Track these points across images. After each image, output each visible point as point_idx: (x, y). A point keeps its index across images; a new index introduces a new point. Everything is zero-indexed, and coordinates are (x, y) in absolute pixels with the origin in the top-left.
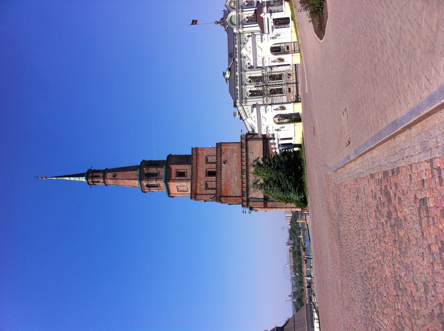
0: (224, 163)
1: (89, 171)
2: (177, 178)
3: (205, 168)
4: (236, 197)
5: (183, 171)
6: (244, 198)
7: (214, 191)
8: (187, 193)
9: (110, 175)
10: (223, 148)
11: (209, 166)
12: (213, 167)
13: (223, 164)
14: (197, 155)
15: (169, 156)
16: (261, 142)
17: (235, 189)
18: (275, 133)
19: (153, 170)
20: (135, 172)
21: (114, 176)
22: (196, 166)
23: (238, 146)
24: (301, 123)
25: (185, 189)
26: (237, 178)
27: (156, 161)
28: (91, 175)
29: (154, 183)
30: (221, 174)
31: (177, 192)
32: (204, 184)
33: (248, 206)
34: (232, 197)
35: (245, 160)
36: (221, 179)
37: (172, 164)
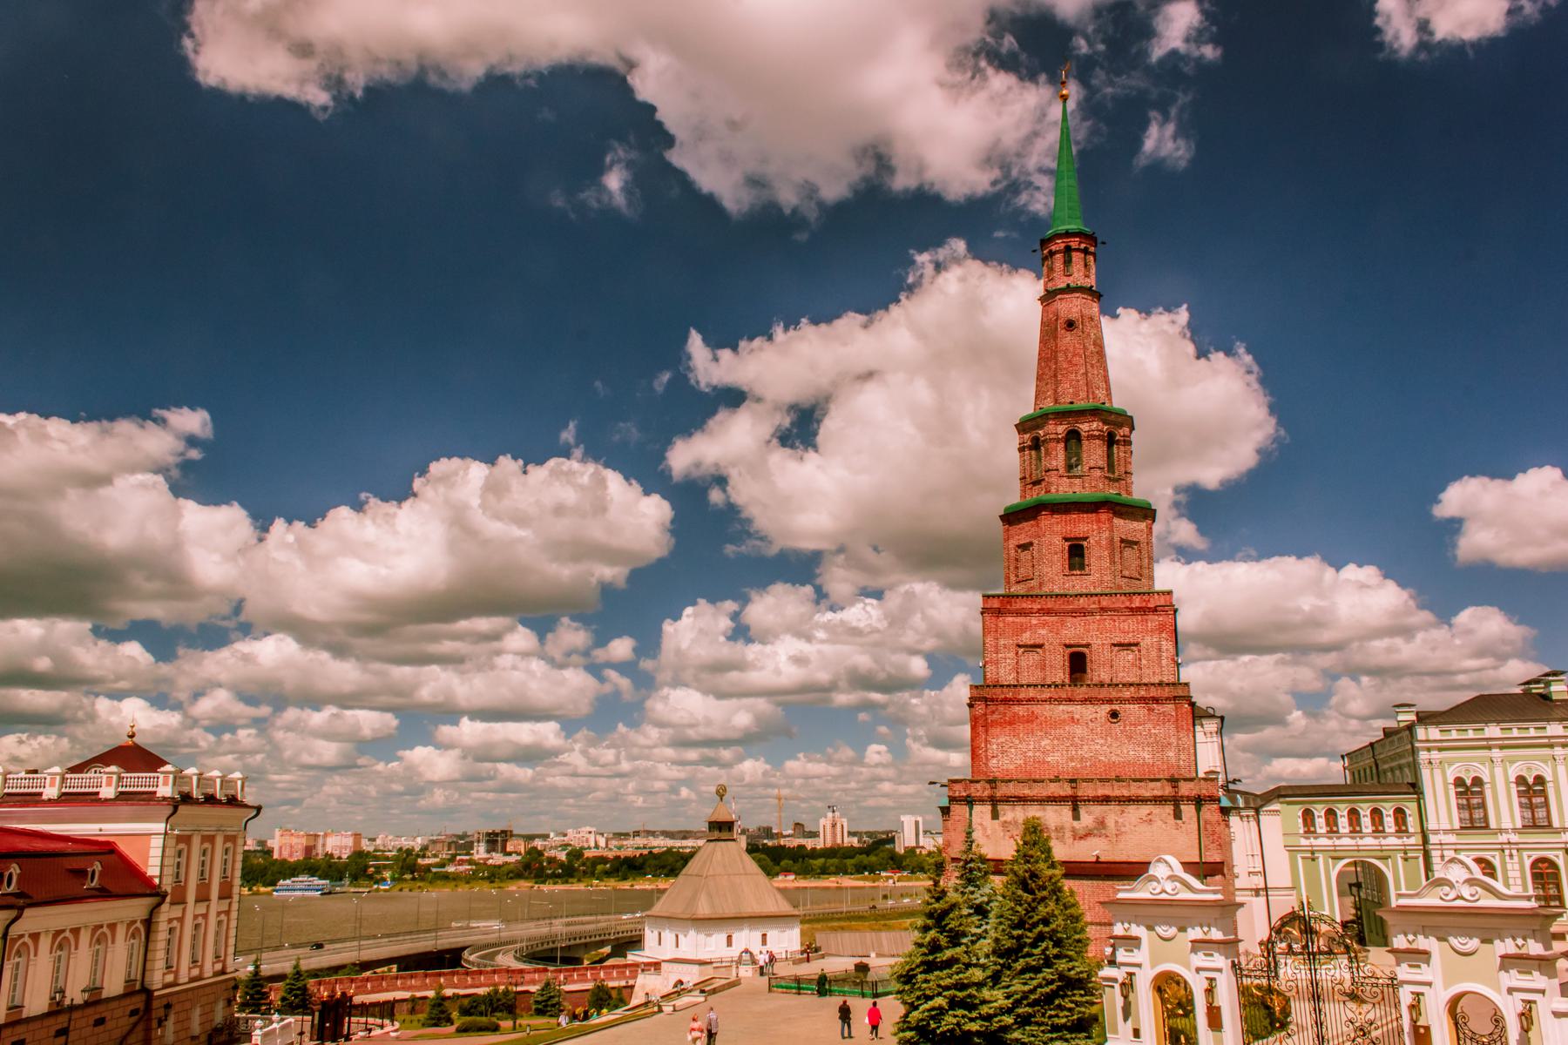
0: (1114, 714)
3: (1096, 643)
6: (978, 786)
8: (1013, 578)
10: (1169, 708)
12: (1099, 672)
13: (1107, 708)
14: (1143, 610)
15: (1146, 513)
19: (1094, 454)
20: (1083, 394)
21: (1070, 325)
28: (1074, 245)
30: (1070, 700)
32: (1039, 641)
33: (952, 799)
35: (1117, 793)
36: (1050, 700)
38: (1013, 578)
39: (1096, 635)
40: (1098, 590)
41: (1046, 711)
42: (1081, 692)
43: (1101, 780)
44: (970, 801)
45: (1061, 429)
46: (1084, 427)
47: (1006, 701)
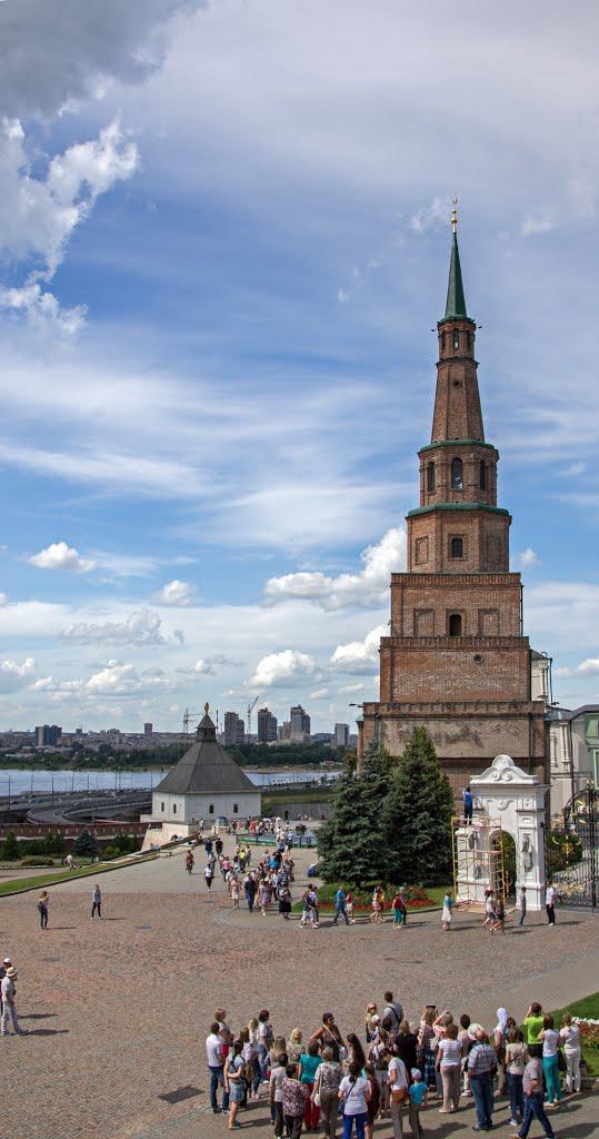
0: (477, 658)
1: (471, 324)
2: (446, 541)
4: (392, 688)
5: (464, 552)
7: (408, 632)
8: (413, 562)
9: (459, 372)
10: (515, 654)
12: (469, 628)
13: (474, 654)
14: (502, 587)
15: (505, 517)
19: (470, 475)
20: (465, 433)
21: (457, 384)
25: (422, 557)
26: (439, 690)
27: (494, 483)
28: (460, 328)
29: (438, 480)
31: (415, 536)
34: (392, 677)
35: (479, 712)
37: (481, 523)
38: (413, 562)
39: (466, 602)
40: (471, 572)
42: (457, 642)
43: (466, 704)
44: (379, 718)
45: (451, 457)
47: (405, 649)
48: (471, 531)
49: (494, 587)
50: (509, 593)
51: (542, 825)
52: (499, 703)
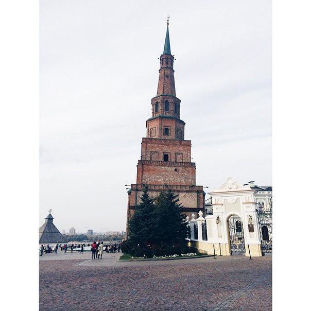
0: (176, 170)
9: (168, 72)
10: (190, 169)
11: (173, 156)
14: (184, 145)
15: (183, 123)
16: (195, 206)
17: (149, 179)
18: (214, 216)
19: (172, 107)
22: (174, 144)
23: (193, 184)
24: (229, 254)
28: (169, 57)
29: (160, 108)
35: (178, 189)
39: (171, 150)
41: (158, 168)
44: (137, 190)
46: (170, 101)
48: (172, 126)
49: (181, 145)
50: (186, 148)
51: (257, 210)
52: (185, 186)
